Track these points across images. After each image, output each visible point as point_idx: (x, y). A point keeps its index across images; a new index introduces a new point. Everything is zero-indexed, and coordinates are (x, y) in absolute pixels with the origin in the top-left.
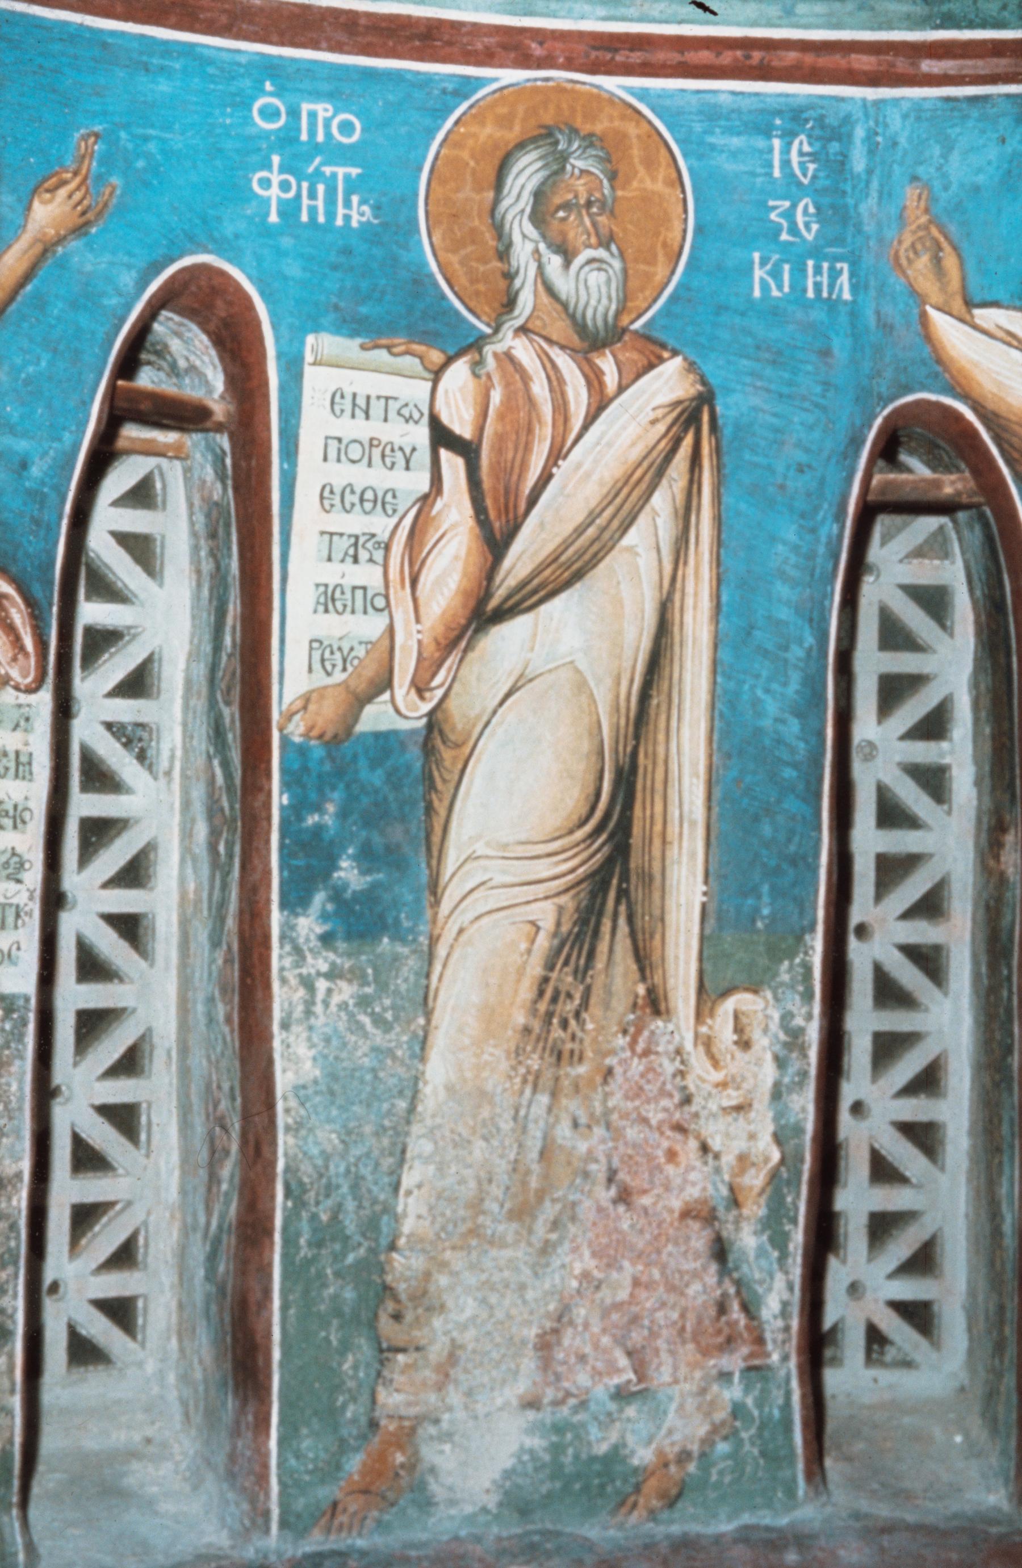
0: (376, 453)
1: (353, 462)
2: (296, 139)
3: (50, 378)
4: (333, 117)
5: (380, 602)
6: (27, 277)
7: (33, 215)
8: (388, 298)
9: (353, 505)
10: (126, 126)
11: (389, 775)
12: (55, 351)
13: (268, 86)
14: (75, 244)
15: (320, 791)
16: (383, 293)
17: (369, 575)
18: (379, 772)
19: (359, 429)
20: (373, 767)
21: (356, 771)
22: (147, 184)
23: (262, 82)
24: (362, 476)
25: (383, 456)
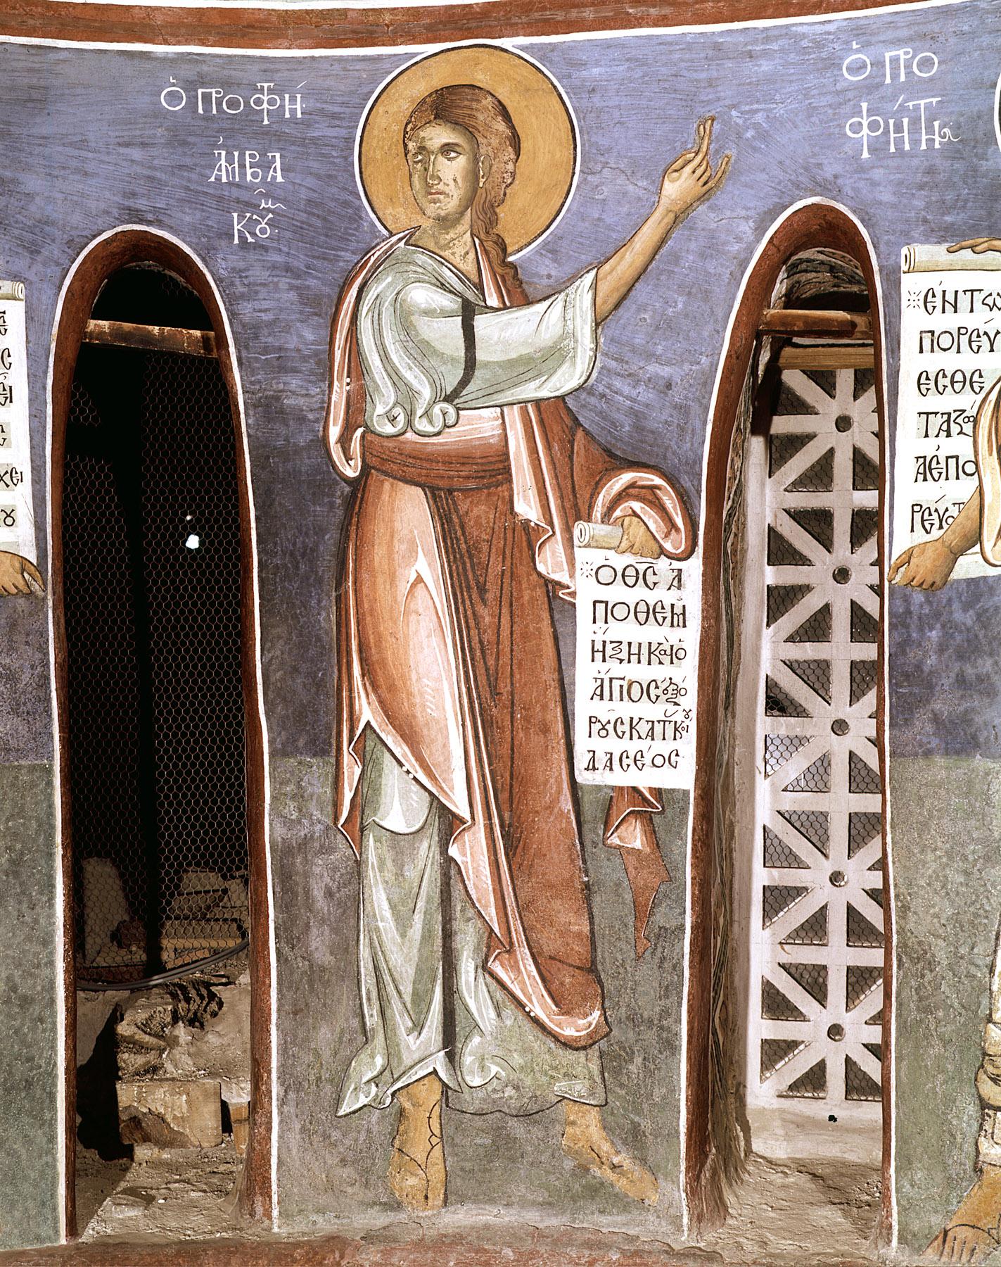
0: (964, 340)
1: (945, 350)
2: (882, 84)
3: (687, 316)
4: (914, 57)
5: (970, 468)
6: (663, 241)
7: (664, 192)
8: (970, 204)
9: (945, 387)
10: (734, 106)
11: (979, 616)
12: (689, 293)
13: (855, 46)
14: (702, 208)
15: (921, 630)
16: (966, 201)
17: (960, 446)
18: (971, 612)
19: (943, 321)
20: (965, 610)
21: (951, 613)
22: (755, 149)
23: (848, 42)
24: (949, 362)
25: (970, 342)
